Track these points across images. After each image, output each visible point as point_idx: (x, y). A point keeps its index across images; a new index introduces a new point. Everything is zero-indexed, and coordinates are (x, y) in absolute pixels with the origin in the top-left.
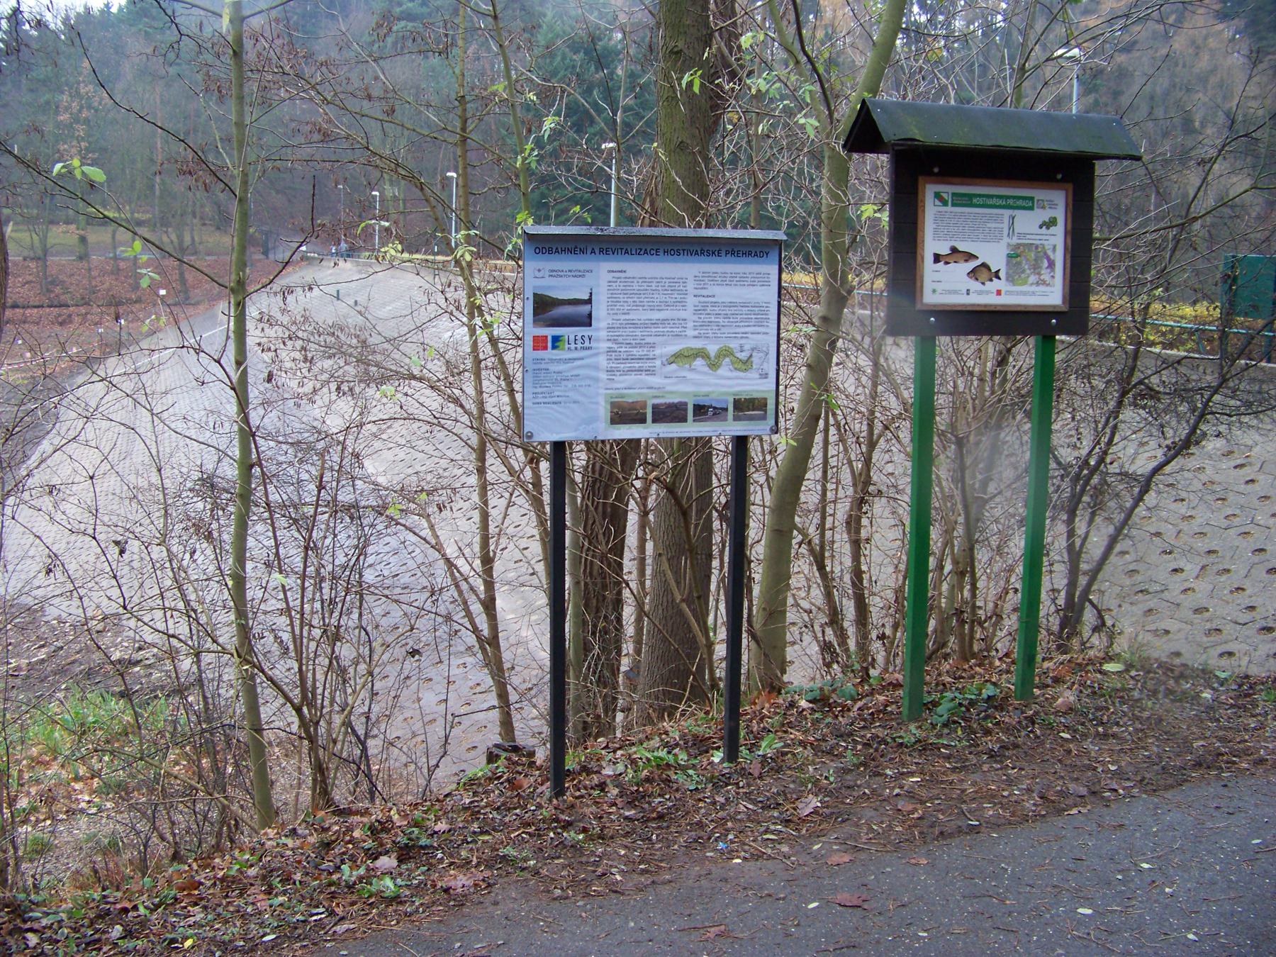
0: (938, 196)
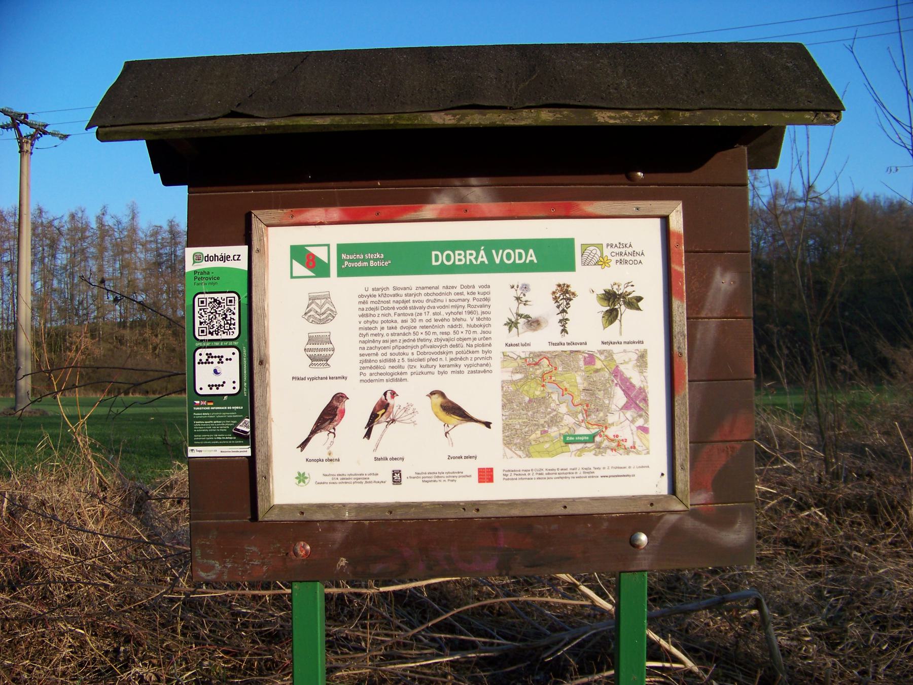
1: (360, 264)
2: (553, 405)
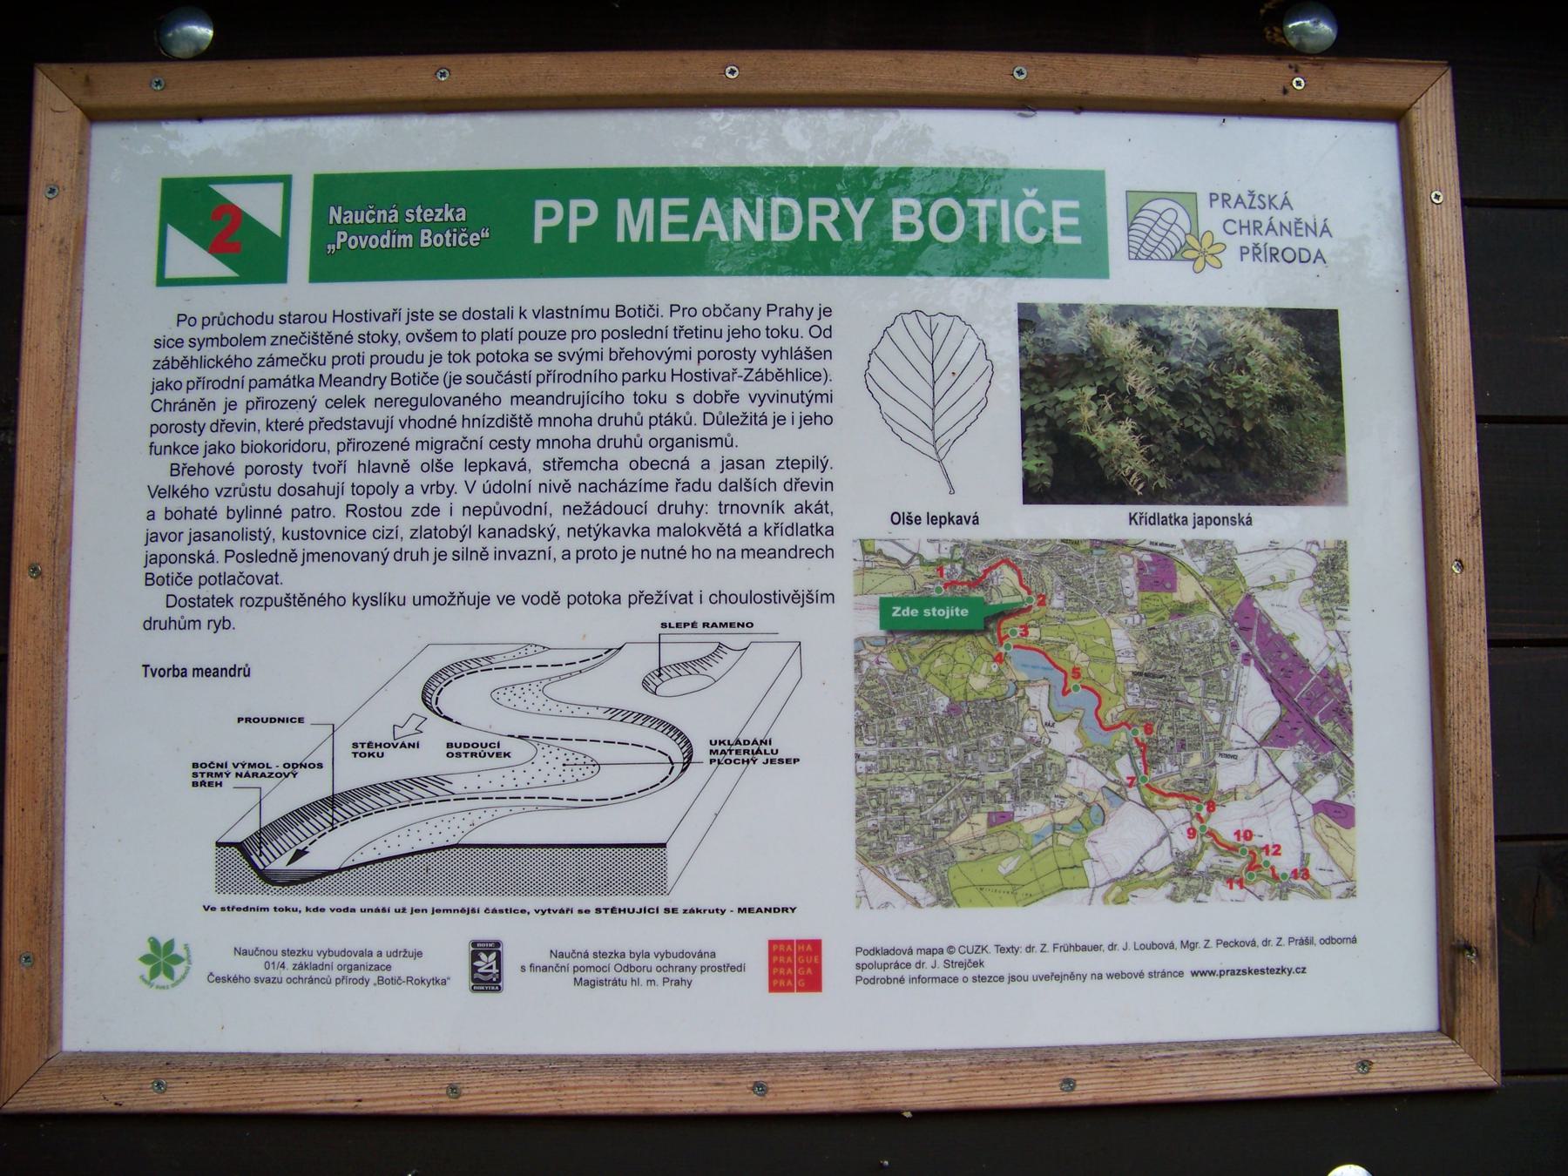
0: (196, 208)
1: (386, 240)
2: (1031, 725)
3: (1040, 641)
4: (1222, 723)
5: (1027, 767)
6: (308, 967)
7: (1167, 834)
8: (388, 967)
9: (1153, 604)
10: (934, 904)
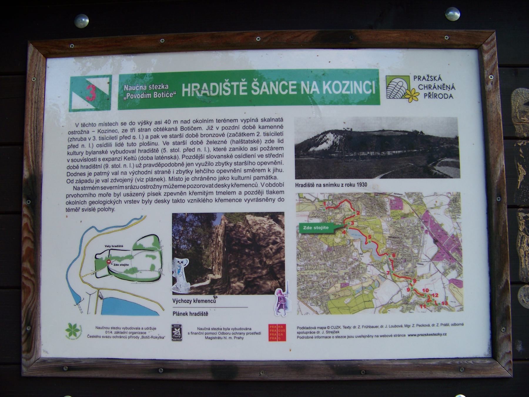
2: (355, 254)
3: (358, 226)
4: (418, 253)
5: (353, 268)
6: (119, 333)
7: (400, 290)
8: (145, 333)
9: (395, 214)
10: (323, 313)
